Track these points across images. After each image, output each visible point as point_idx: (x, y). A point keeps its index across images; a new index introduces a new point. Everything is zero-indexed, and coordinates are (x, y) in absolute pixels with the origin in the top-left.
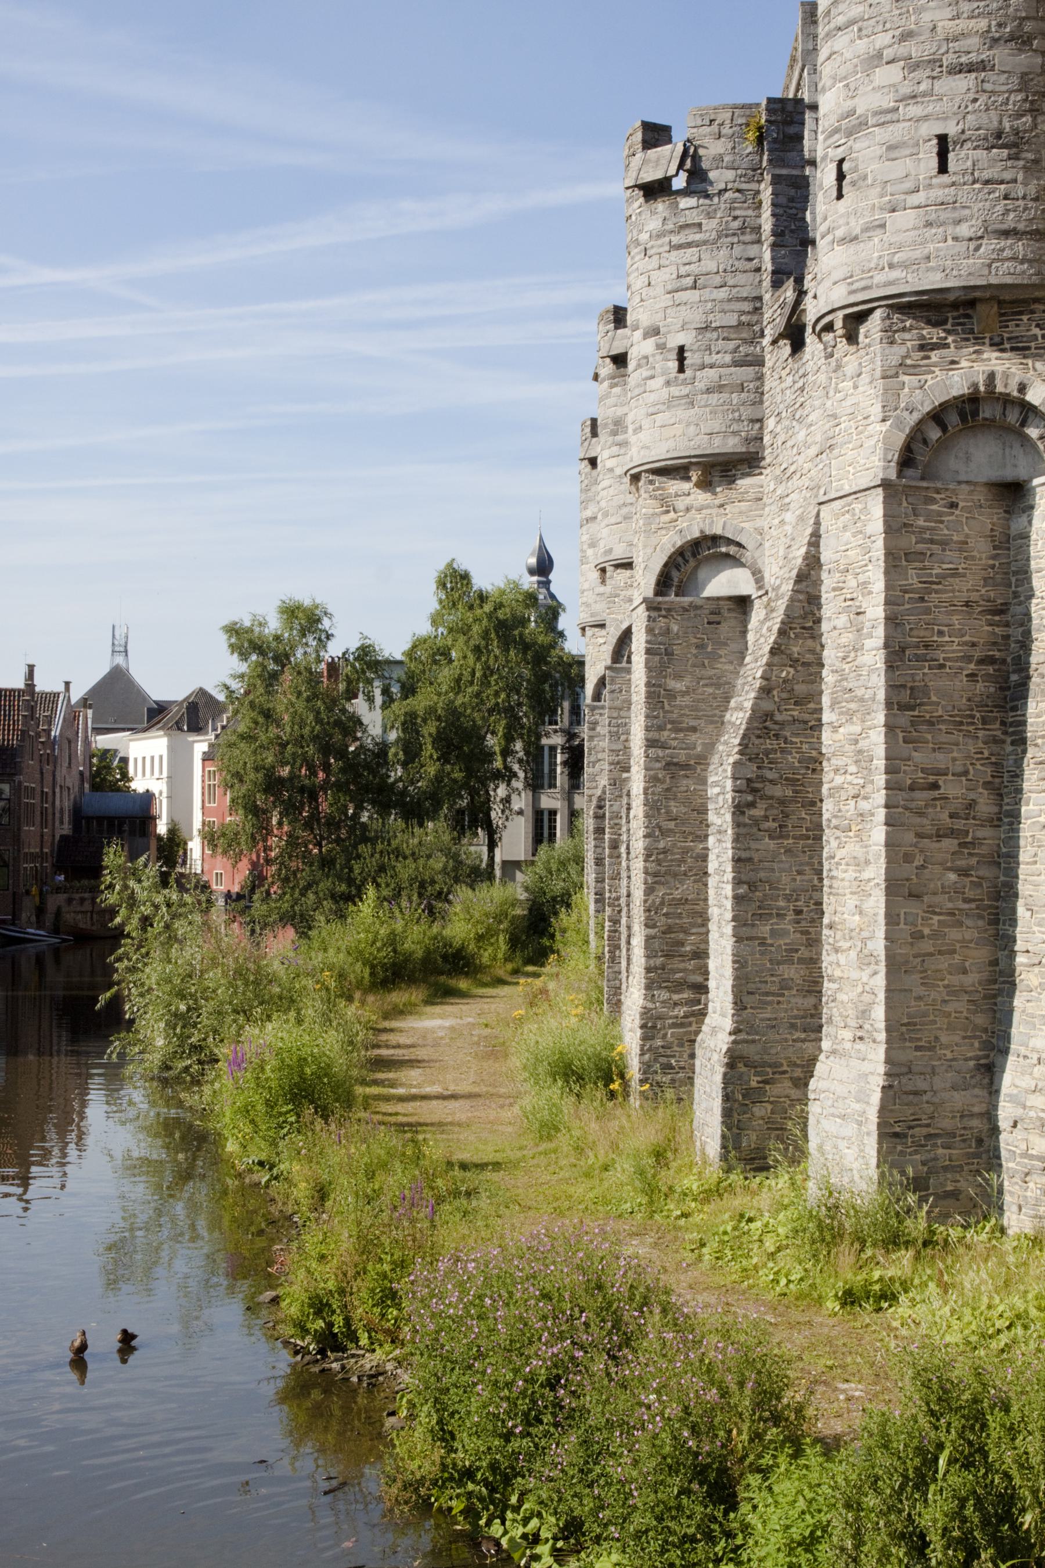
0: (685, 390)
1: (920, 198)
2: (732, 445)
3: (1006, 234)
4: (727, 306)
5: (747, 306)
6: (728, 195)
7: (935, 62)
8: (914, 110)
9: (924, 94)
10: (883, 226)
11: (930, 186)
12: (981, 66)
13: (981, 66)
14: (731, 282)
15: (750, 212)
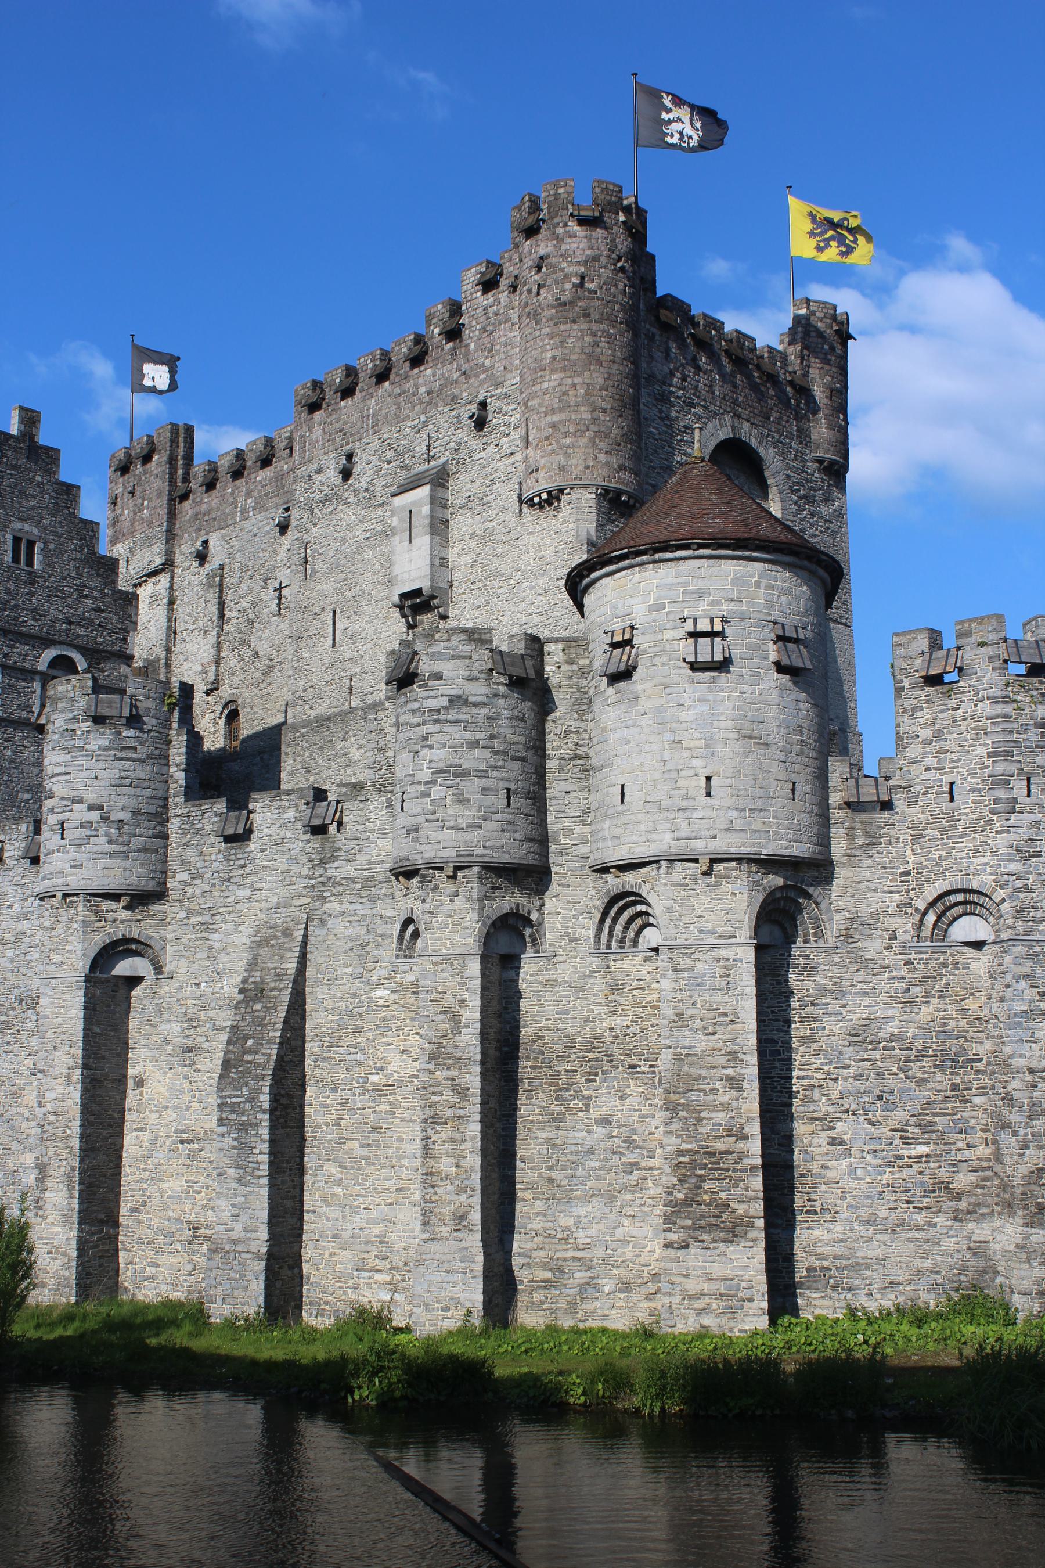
0: (125, 848)
1: (499, 816)
2: (151, 886)
3: (532, 840)
4: (151, 801)
5: (161, 803)
6: (152, 733)
7: (505, 753)
8: (495, 774)
9: (501, 767)
10: (480, 827)
11: (503, 812)
12: (522, 759)
13: (522, 759)
14: (153, 787)
15: (164, 746)
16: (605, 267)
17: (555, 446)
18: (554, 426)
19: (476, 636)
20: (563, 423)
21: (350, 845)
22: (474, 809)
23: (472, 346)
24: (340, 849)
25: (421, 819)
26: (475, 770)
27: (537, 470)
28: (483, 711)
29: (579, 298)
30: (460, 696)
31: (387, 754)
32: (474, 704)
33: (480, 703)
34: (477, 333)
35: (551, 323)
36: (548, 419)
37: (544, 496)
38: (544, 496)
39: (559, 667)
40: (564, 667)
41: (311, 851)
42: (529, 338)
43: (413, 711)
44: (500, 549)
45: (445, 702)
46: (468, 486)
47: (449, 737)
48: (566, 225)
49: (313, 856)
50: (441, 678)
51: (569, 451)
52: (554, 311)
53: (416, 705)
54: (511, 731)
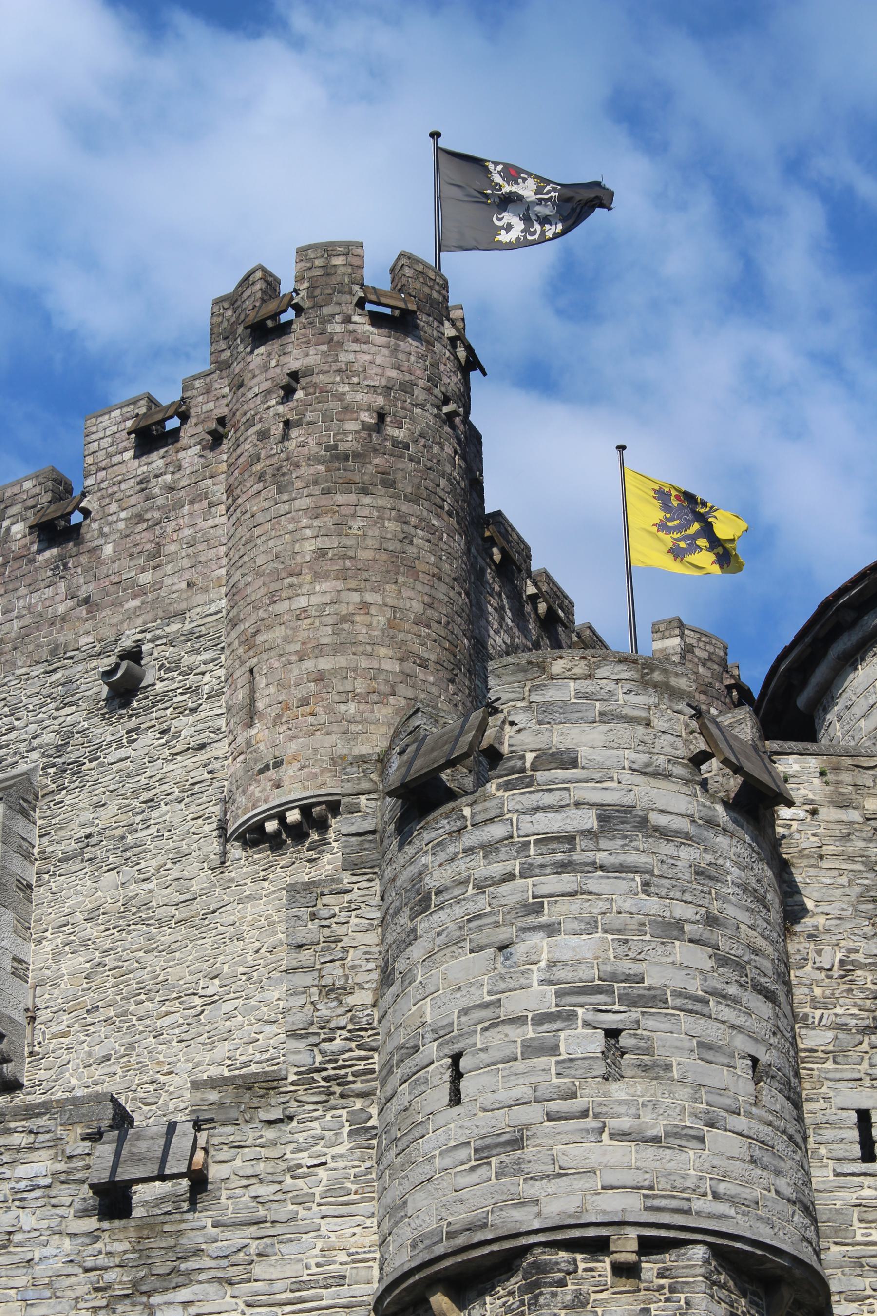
8: (726, 1013)
9: (736, 1000)
10: (701, 1140)
16: (422, 406)
17: (323, 717)
18: (320, 678)
19: (657, 676)
20: (343, 673)
21: (235, 1238)
22: (684, 1092)
23: (108, 550)
24: (198, 1252)
25: (533, 1113)
26: (678, 994)
27: (278, 764)
28: (687, 854)
29: (375, 451)
30: (628, 809)
31: (350, 1000)
32: (663, 833)
33: (677, 833)
34: (121, 525)
35: (316, 490)
36: (309, 664)
37: (293, 816)
38: (293, 816)
39: (814, 812)
40: (827, 813)
41: (102, 1261)
42: (260, 518)
43: (489, 849)
44: (166, 936)
45: (589, 820)
46: (88, 816)
47: (602, 906)
48: (347, 320)
49: (110, 1276)
50: (573, 763)
51: (353, 728)
52: (321, 468)
53: (497, 831)
54: (744, 917)
